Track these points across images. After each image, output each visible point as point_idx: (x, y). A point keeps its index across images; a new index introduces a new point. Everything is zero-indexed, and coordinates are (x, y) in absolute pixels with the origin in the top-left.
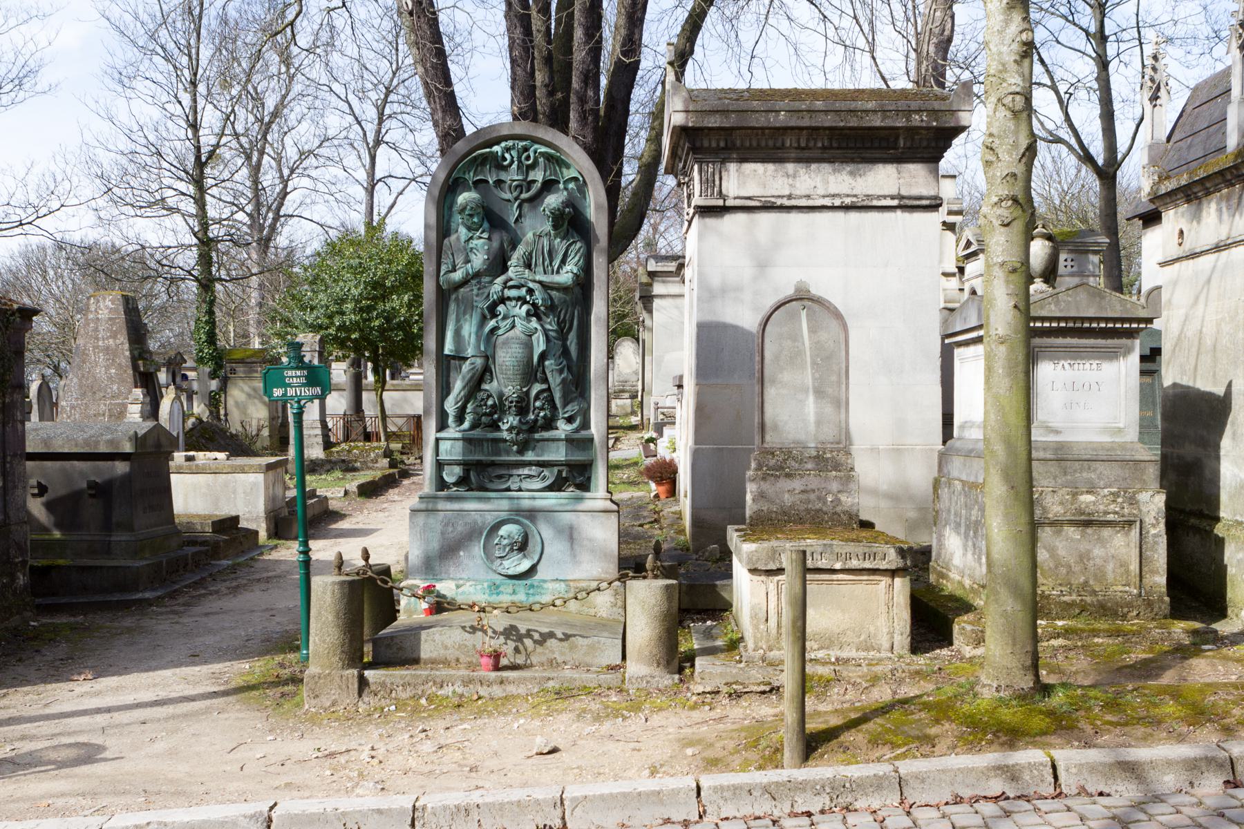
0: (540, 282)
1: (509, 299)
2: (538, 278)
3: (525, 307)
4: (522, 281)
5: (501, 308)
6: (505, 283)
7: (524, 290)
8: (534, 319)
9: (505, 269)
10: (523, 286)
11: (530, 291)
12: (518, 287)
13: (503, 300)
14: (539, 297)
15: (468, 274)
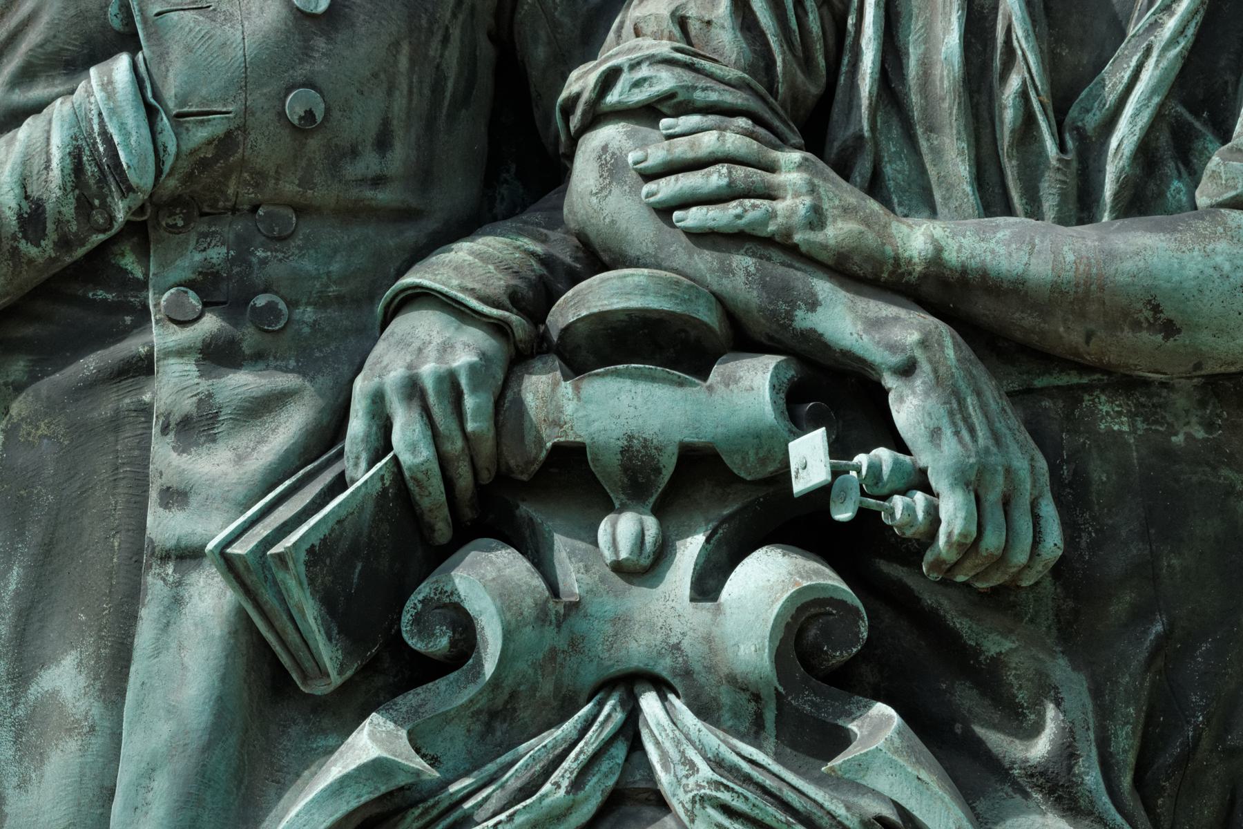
0: (941, 292)
1: (575, 479)
2: (916, 238)
3: (768, 579)
4: (740, 274)
5: (485, 580)
6: (537, 293)
7: (749, 388)
8: (878, 725)
9: (518, 161)
10: (743, 337)
11: (839, 394)
12: (671, 345)
13: (518, 488)
14: (939, 456)
15: (92, 169)
